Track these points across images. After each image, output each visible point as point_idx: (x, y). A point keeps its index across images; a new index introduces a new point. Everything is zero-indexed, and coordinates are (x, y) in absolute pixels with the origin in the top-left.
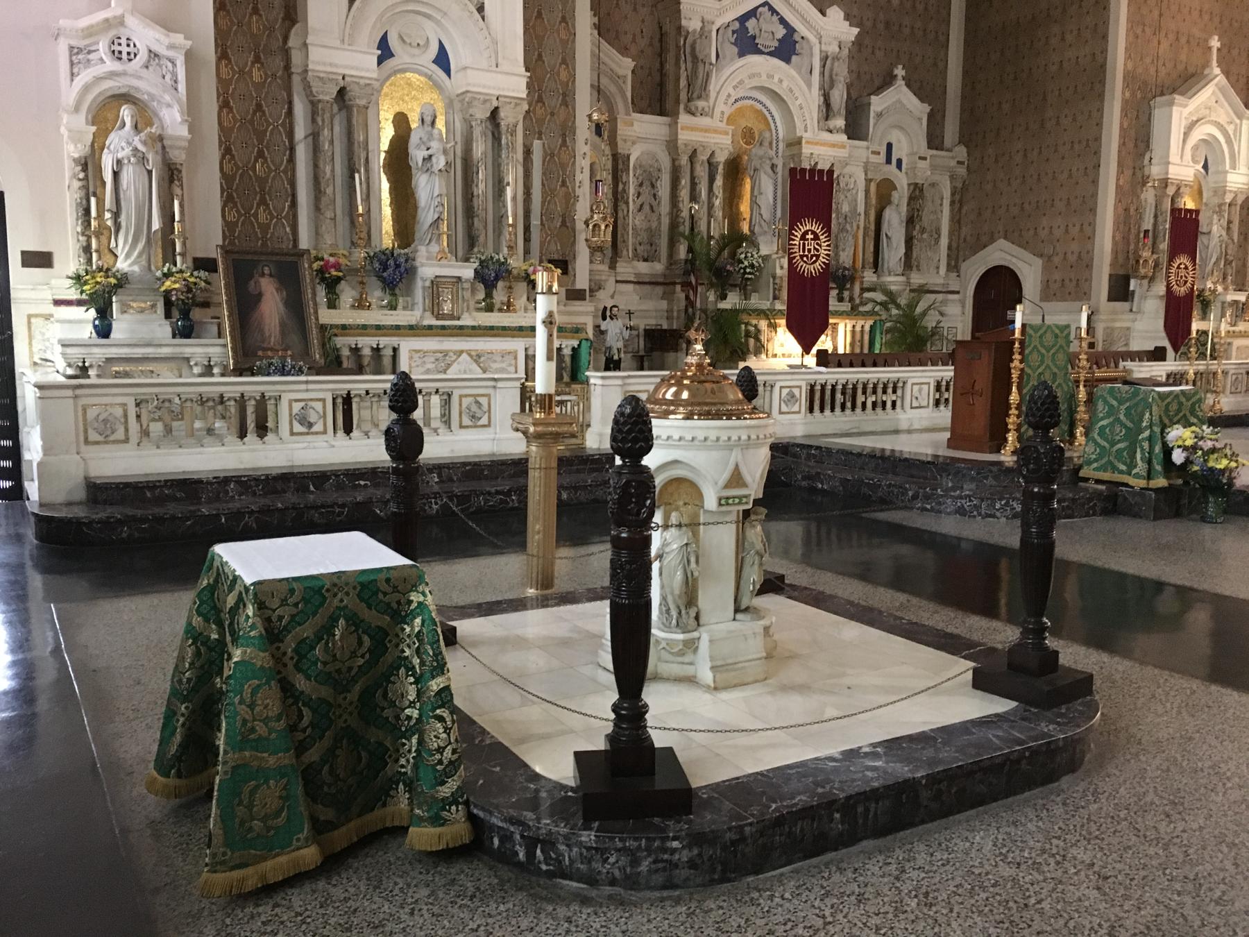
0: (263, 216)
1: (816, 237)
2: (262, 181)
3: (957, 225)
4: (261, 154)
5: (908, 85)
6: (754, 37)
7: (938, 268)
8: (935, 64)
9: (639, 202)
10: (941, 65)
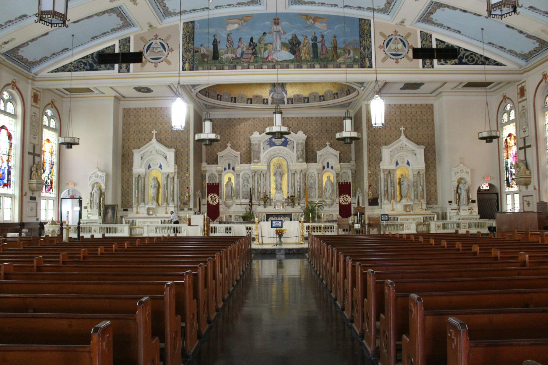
0: (128, 198)
1: (215, 197)
2: (128, 192)
4: (128, 187)
5: (330, 147)
6: (274, 142)
9: (244, 185)
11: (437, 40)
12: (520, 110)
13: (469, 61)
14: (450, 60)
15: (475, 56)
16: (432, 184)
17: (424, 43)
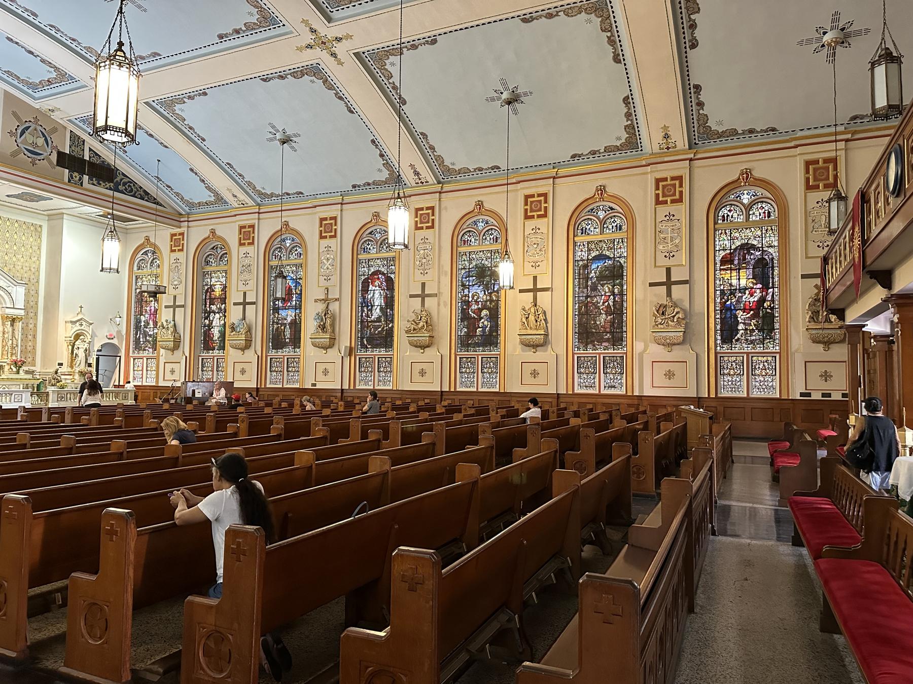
11: (90, 150)
12: (171, 263)
13: (126, 189)
14: (104, 182)
15: (134, 185)
16: (30, 337)
17: (73, 148)
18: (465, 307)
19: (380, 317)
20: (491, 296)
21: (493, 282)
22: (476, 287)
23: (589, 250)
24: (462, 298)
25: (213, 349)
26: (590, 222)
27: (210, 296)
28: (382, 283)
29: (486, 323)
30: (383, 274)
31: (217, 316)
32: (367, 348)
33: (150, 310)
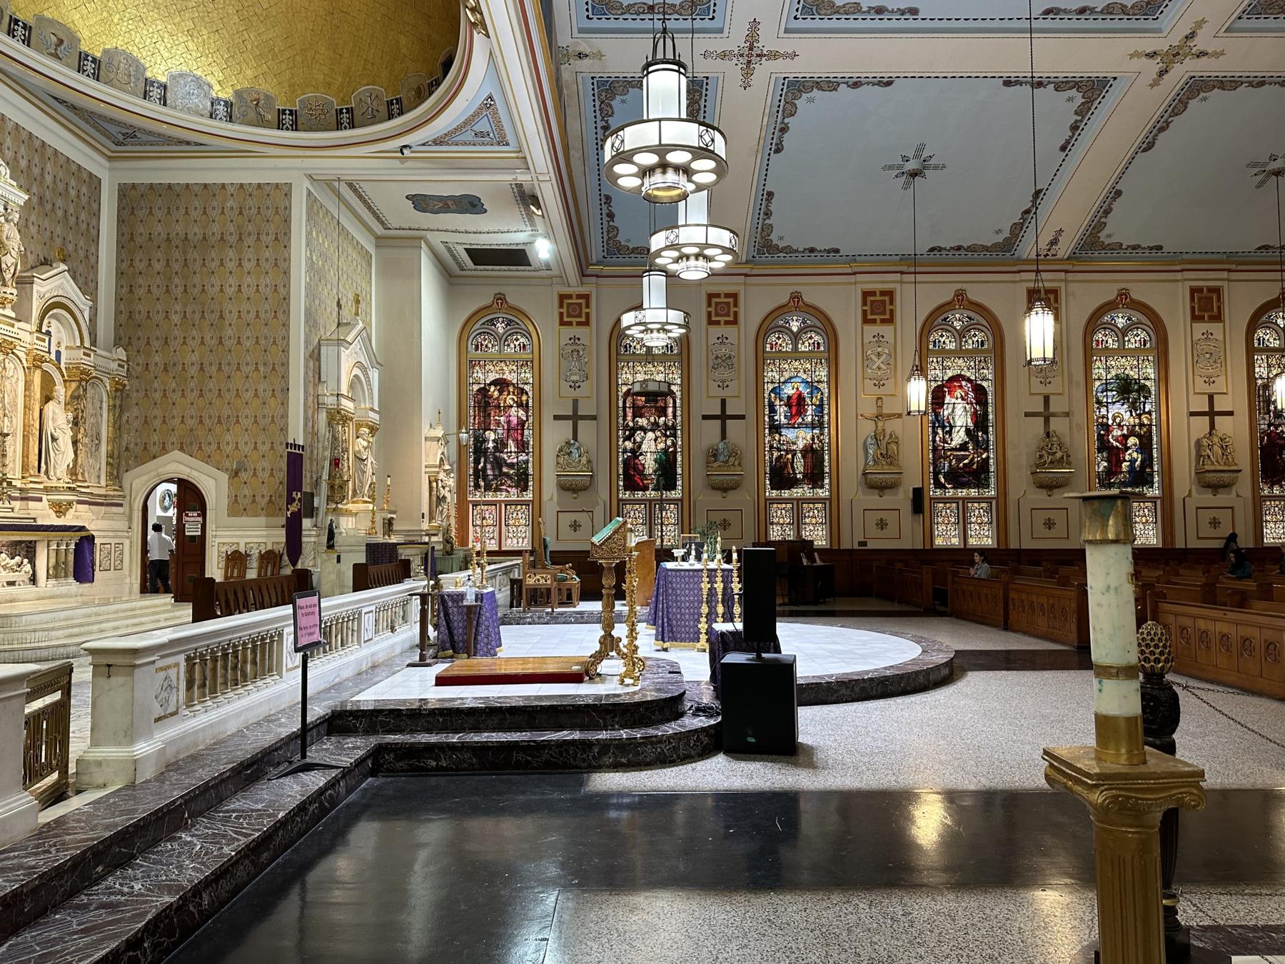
3: (118, 431)
7: (99, 477)
8: (87, 257)
10: (93, 259)
12: (562, 344)
18: (1102, 432)
19: (966, 443)
20: (1140, 419)
21: (1142, 399)
22: (1118, 405)
23: (1269, 366)
24: (1097, 419)
25: (645, 489)
26: (1268, 332)
27: (634, 404)
28: (967, 394)
29: (1135, 455)
30: (969, 380)
31: (650, 435)
32: (946, 488)
33: (509, 422)
